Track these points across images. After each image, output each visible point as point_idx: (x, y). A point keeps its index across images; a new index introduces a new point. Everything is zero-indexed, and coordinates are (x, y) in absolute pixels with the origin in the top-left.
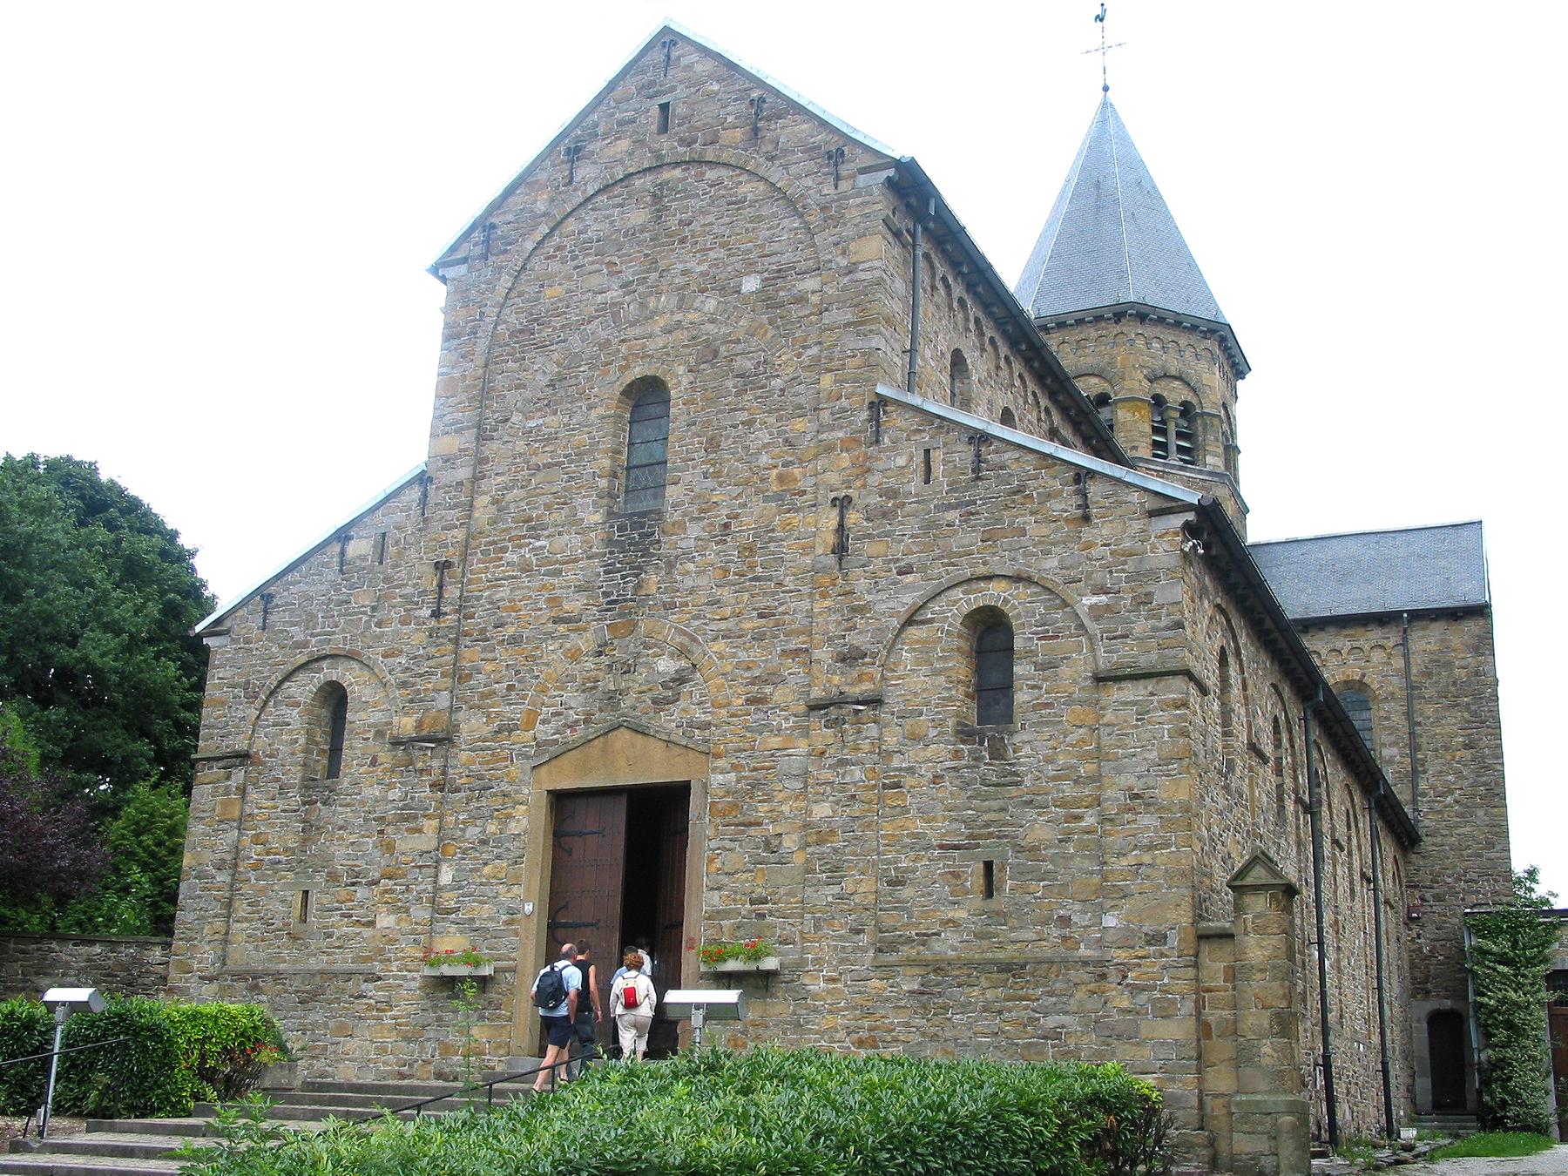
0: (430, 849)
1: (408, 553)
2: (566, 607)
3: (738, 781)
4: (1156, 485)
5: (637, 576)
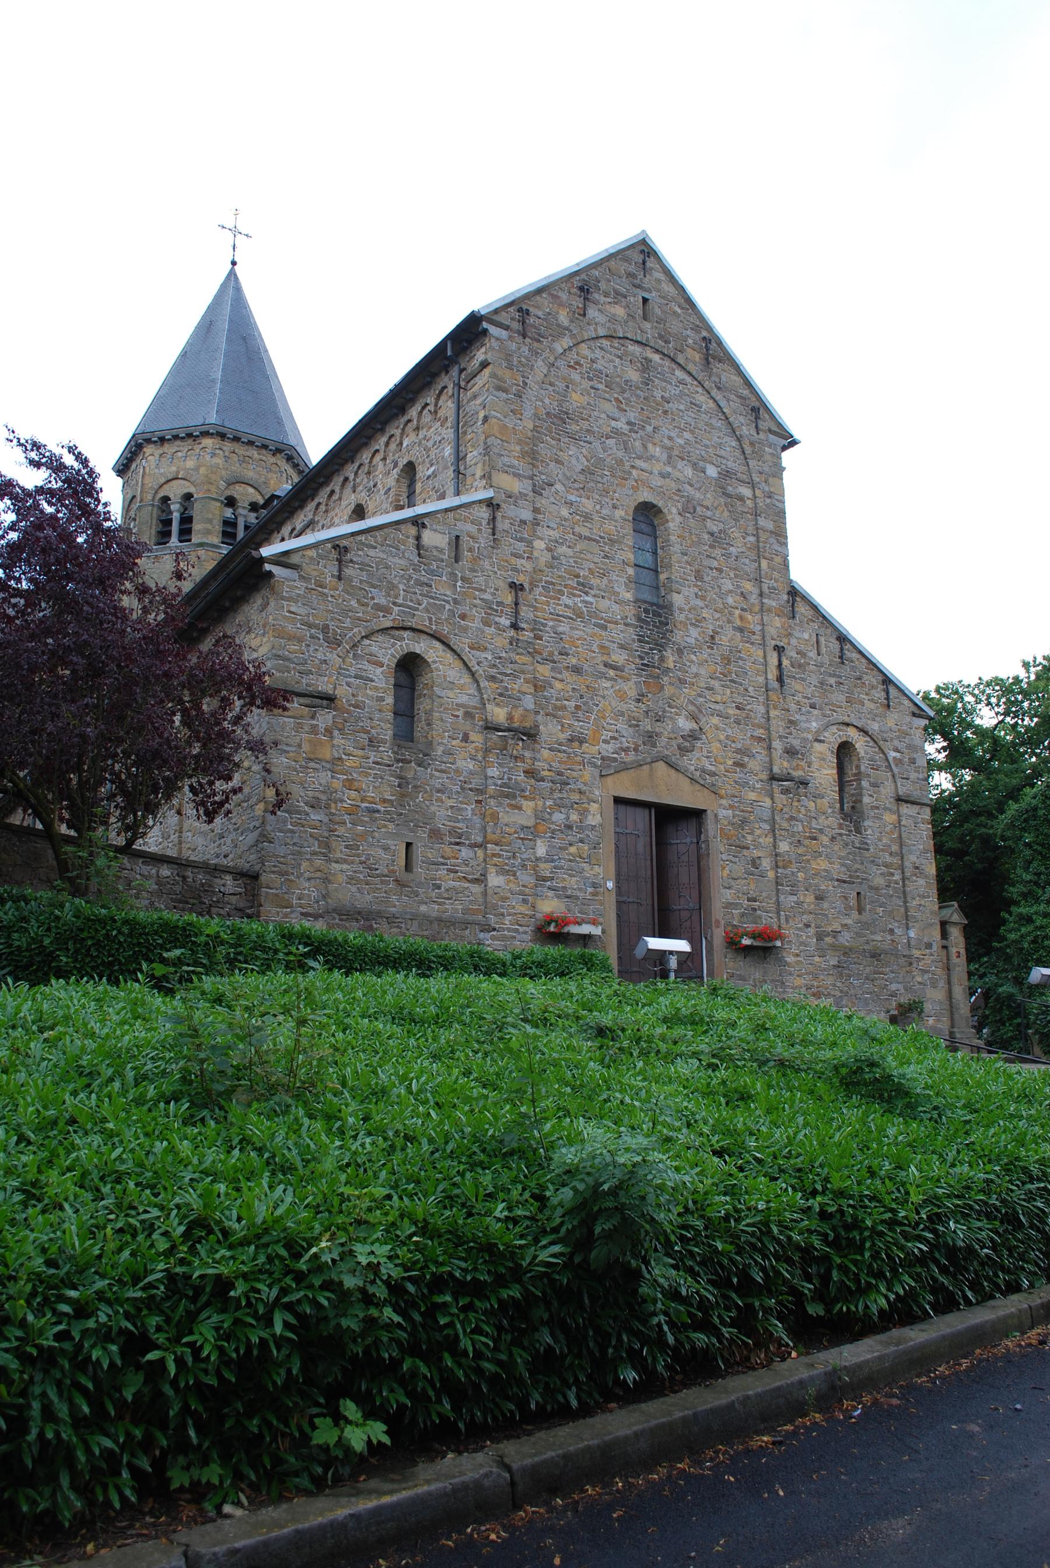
0: (530, 824)
1: (482, 562)
2: (613, 657)
3: (734, 817)
5: (660, 651)
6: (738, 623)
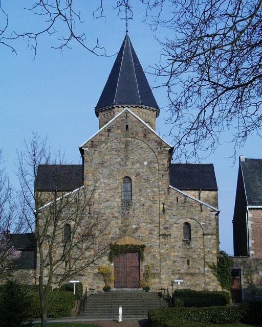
4: (212, 207)
6: (152, 199)
